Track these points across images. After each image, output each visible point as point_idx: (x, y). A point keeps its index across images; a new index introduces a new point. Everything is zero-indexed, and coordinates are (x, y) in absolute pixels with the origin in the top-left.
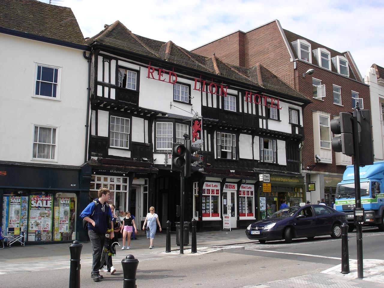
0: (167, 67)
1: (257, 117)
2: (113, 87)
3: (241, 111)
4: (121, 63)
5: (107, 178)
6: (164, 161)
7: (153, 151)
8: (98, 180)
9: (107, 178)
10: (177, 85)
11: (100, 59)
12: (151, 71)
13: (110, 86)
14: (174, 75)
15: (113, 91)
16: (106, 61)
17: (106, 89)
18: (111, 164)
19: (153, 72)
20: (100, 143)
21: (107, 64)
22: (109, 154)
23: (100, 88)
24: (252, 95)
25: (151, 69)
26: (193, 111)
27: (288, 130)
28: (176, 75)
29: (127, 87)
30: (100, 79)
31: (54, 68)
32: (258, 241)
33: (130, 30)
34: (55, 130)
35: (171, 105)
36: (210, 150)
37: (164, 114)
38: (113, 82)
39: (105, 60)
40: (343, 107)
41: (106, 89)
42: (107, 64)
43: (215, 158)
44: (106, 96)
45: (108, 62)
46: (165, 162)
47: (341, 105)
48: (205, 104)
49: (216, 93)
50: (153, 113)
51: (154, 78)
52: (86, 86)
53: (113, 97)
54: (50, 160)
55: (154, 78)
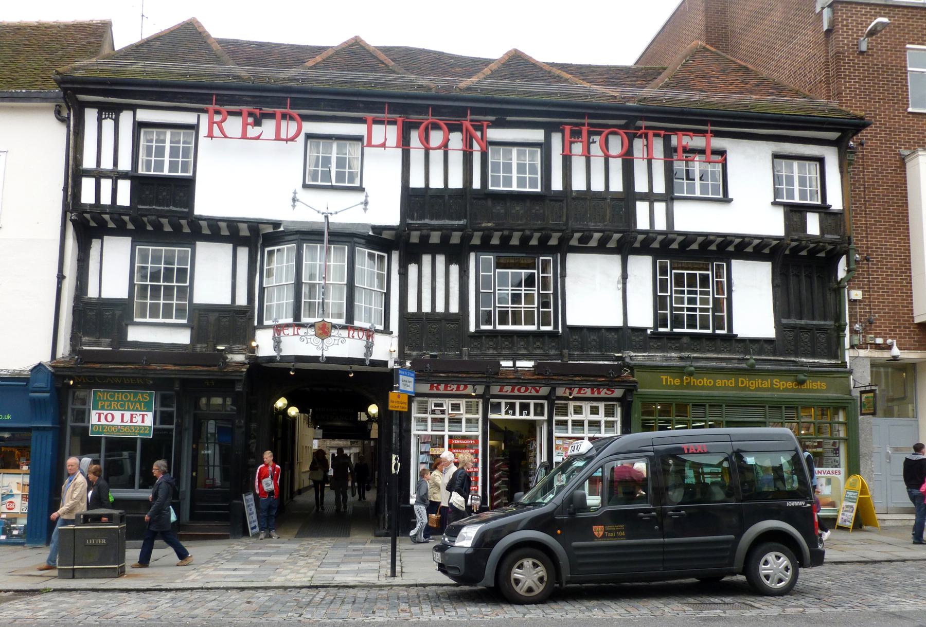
0: (269, 100)
1: (629, 197)
2: (124, 175)
4: (144, 115)
6: (364, 350)
7: (256, 324)
11: (91, 116)
12: (217, 118)
13: (116, 176)
14: (292, 118)
15: (125, 187)
16: (106, 118)
17: (106, 184)
19: (224, 120)
21: (108, 124)
23: (88, 184)
25: (217, 112)
26: (297, 203)
28: (298, 118)
30: (89, 162)
36: (454, 308)
37: (276, 224)
38: (125, 164)
39: (103, 116)
41: (106, 184)
42: (108, 124)
43: (472, 328)
44: (106, 200)
45: (111, 118)
46: (365, 355)
48: (417, 181)
51: (226, 137)
53: (124, 199)
55: (226, 137)
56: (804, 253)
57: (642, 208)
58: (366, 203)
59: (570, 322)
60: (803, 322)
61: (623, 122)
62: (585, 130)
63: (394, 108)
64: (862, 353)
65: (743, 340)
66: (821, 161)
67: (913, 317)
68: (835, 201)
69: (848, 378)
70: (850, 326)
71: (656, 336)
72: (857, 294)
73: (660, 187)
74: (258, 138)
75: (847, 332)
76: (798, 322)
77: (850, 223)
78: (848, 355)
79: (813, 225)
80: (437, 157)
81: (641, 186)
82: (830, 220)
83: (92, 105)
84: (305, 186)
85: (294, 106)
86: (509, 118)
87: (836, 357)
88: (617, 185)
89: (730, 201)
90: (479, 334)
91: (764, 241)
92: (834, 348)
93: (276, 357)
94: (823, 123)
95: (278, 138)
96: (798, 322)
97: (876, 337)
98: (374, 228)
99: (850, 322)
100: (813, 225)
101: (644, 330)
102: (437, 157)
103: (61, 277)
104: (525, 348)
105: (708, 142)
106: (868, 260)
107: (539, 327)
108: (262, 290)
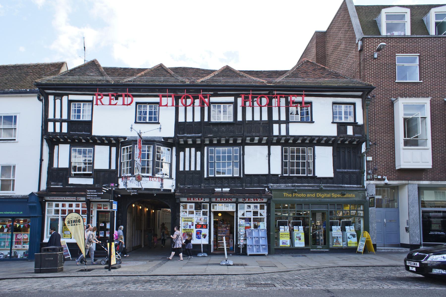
0: (119, 89)
1: (271, 122)
2: (65, 121)
3: (206, 119)
4: (72, 97)
5: (72, 204)
6: (160, 186)
7: (118, 176)
8: (79, 207)
9: (59, 204)
10: (88, 104)
11: (51, 98)
12: (99, 97)
13: (61, 121)
14: (129, 96)
15: (65, 125)
16: (57, 99)
17: (58, 124)
18: (195, 193)
19: (102, 98)
20: (61, 173)
21: (58, 101)
22: (70, 182)
23: (51, 125)
24: (253, 98)
25: (99, 95)
26: (132, 129)
27: (332, 131)
28: (131, 96)
29: (212, 121)
30: (51, 116)
31: (13, 115)
32: (422, 262)
33: (151, 64)
34: (14, 167)
35: (131, 128)
36: (198, 168)
37: (125, 138)
38: (65, 117)
39: (56, 98)
40: (421, 83)
41: (58, 124)
42: (58, 101)
43: (205, 176)
44: (58, 130)
45: (59, 99)
46: (161, 187)
47: (419, 81)
48: (181, 119)
49: (267, 106)
50: (333, 139)
51: (103, 104)
52: (41, 125)
53: (65, 130)
54: (11, 192)
55: (103, 104)
56: (347, 142)
57: (276, 126)
58: (160, 129)
59: (246, 173)
60: (346, 170)
61: (267, 92)
62: (250, 96)
63: (171, 91)
64: (372, 182)
65: (320, 178)
66: (354, 104)
67: (395, 167)
68: (360, 121)
69: (365, 192)
70: (367, 171)
71: (282, 177)
72: (370, 159)
73: (283, 118)
74: (115, 104)
75: (365, 174)
76: (343, 170)
77: (366, 130)
78: (366, 183)
79: (350, 131)
80: (190, 109)
81: (275, 117)
82: (358, 128)
83: (51, 94)
84: (136, 122)
85: (130, 91)
86: (219, 93)
87: (360, 184)
88: (265, 117)
89: (312, 122)
90: (208, 178)
91: (329, 138)
92: (360, 181)
93: (125, 188)
94: (354, 88)
95: (124, 104)
96: (343, 170)
97: (378, 176)
98: (164, 138)
99: (367, 170)
100: (350, 131)
101: (277, 175)
102: (190, 109)
103: (41, 160)
104: (227, 184)
105: (303, 99)
106: (375, 144)
107: (233, 175)
108: (121, 163)
